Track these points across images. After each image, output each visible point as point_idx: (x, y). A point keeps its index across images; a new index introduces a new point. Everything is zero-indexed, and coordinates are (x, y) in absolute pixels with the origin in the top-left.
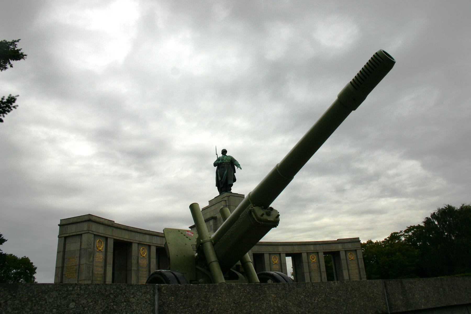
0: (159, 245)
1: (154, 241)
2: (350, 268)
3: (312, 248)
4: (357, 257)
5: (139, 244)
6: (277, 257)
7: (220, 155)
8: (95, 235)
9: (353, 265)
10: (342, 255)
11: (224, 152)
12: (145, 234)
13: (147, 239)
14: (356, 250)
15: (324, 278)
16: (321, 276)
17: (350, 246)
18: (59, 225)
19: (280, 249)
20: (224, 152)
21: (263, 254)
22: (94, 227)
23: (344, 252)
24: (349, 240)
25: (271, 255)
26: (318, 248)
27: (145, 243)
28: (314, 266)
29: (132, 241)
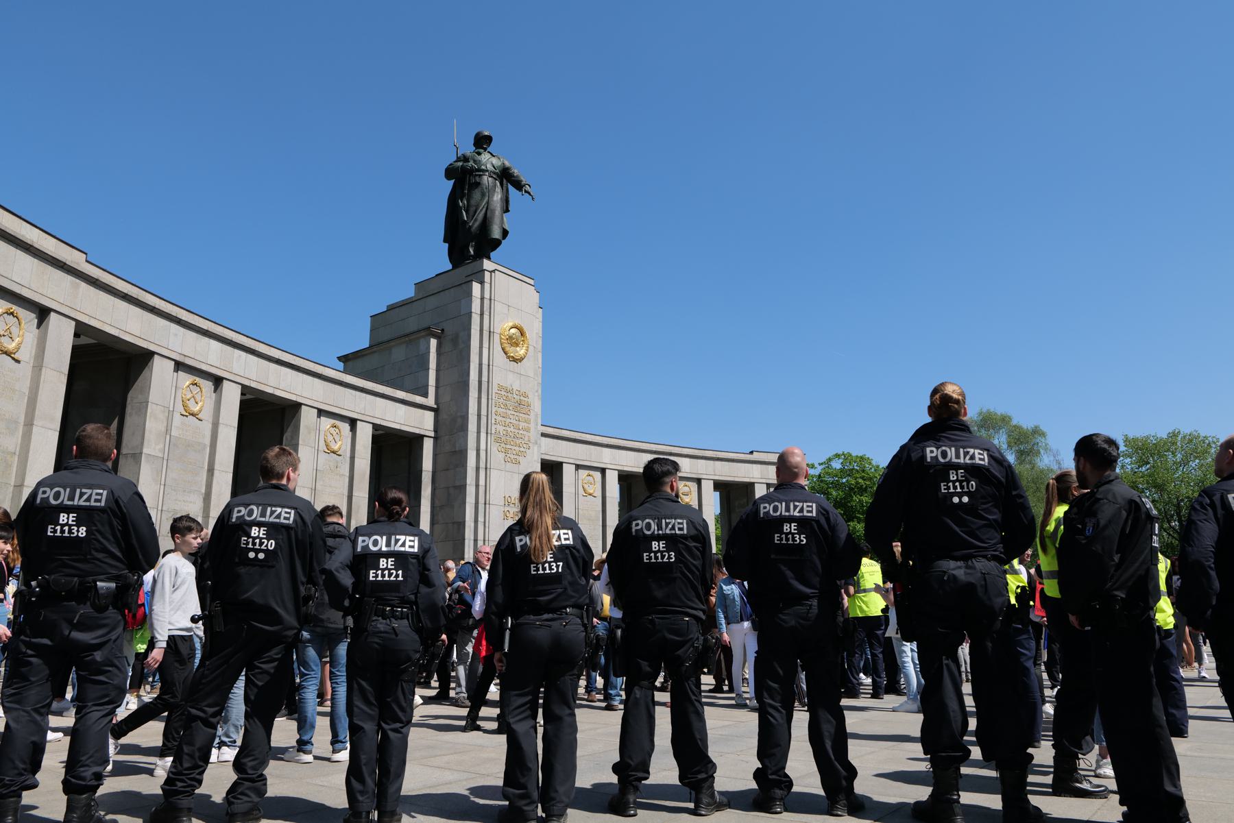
0: (254, 385)
11: (482, 141)
13: (211, 355)
20: (482, 141)
21: (561, 464)
25: (580, 471)
27: (204, 367)
29: (152, 348)
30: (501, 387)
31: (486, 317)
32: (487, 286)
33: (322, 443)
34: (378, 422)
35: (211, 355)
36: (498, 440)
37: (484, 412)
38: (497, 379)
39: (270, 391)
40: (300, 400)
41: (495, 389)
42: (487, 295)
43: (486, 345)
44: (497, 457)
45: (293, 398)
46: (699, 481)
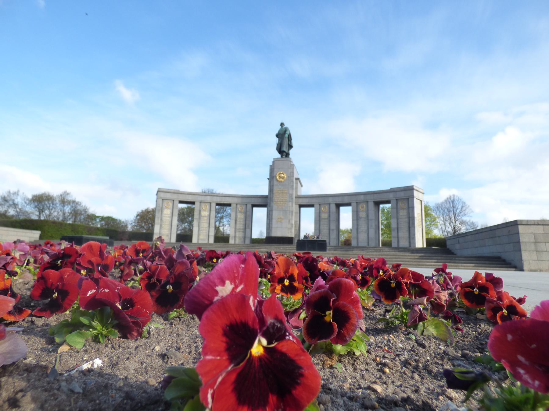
2: (400, 217)
3: (362, 198)
4: (409, 205)
5: (200, 202)
6: (327, 207)
7: (280, 127)
8: (163, 199)
11: (282, 124)
13: (208, 199)
14: (408, 199)
16: (368, 224)
17: (402, 195)
19: (330, 200)
22: (162, 195)
23: (395, 201)
26: (368, 197)
28: (362, 214)
44: (275, 207)
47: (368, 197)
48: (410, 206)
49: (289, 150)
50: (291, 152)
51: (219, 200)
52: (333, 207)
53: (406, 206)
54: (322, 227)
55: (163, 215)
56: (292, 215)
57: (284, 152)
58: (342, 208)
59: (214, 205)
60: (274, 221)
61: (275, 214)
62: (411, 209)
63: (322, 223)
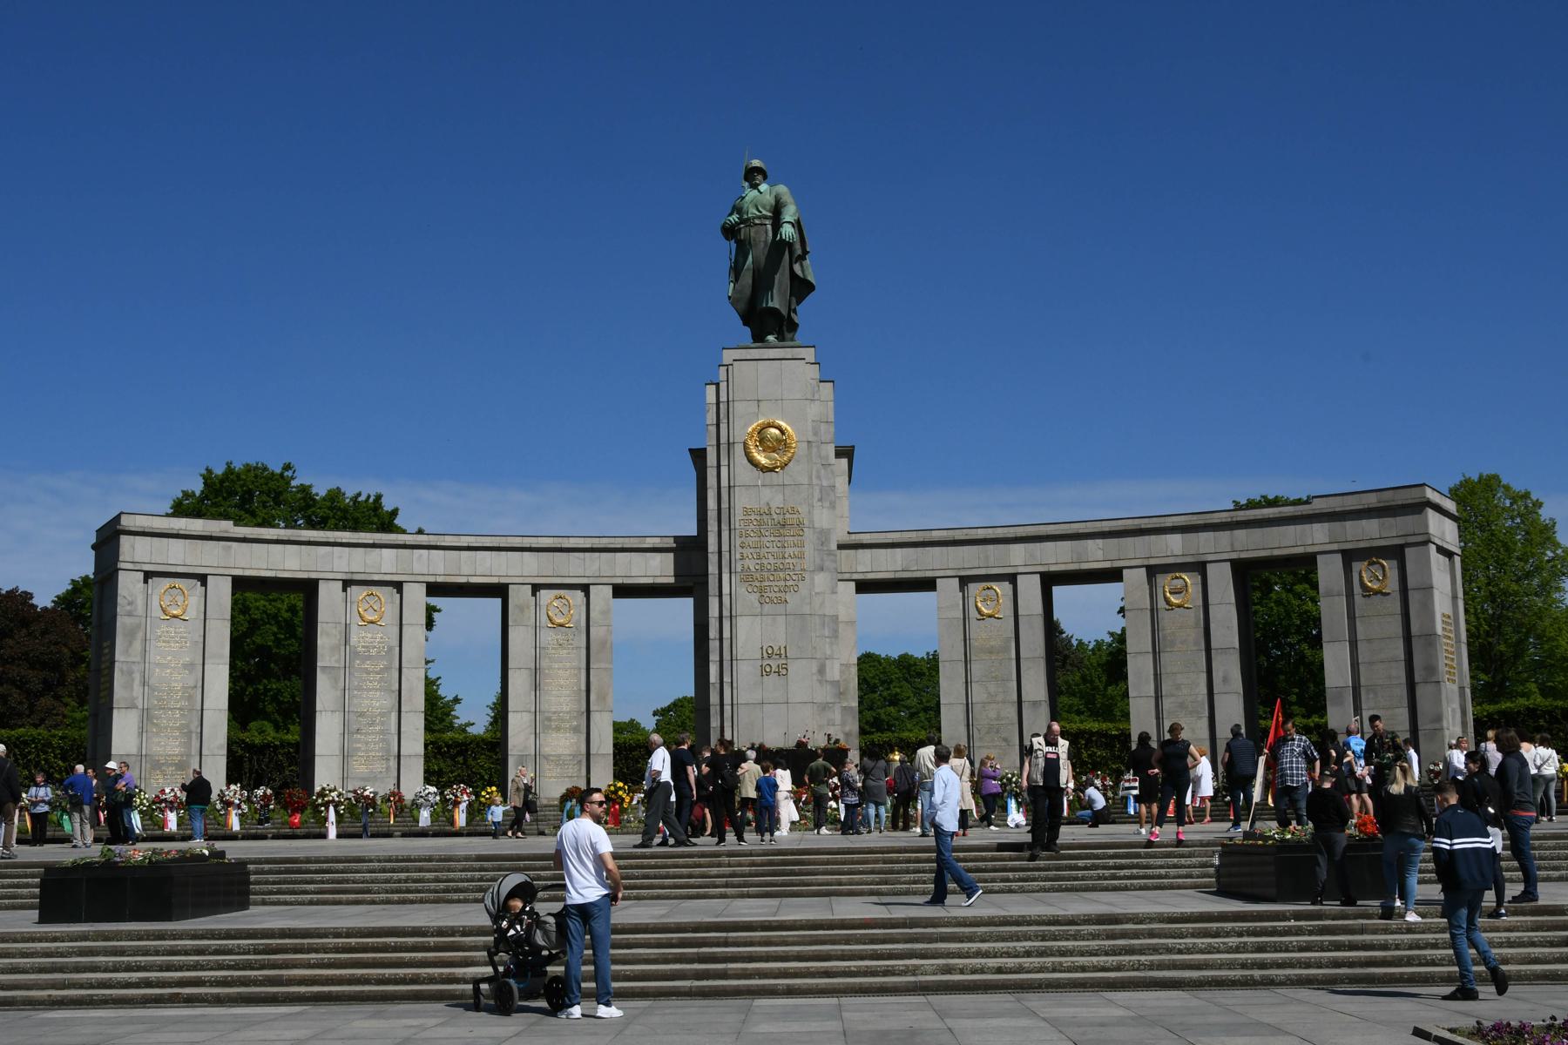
0: (440, 579)
1: (417, 568)
3: (1173, 547)
5: (347, 584)
8: (148, 575)
9: (1381, 624)
10: (1329, 572)
12: (374, 546)
13: (386, 563)
15: (1225, 680)
17: (1370, 531)
18: (94, 547)
24: (1371, 501)
25: (974, 588)
27: (376, 578)
29: (314, 576)
30: (746, 511)
31: (723, 427)
32: (723, 386)
33: (544, 618)
34: (619, 581)
35: (386, 563)
36: (748, 578)
37: (725, 547)
38: (742, 500)
39: (463, 580)
40: (503, 580)
41: (738, 515)
42: (723, 398)
43: (724, 462)
45: (495, 580)
46: (1200, 568)
47: (1205, 544)
48: (1411, 583)
49: (791, 310)
50: (805, 313)
51: (441, 566)
52: (1030, 589)
53: (1392, 584)
54: (978, 694)
55: (154, 657)
56: (835, 635)
57: (774, 312)
58: (1058, 591)
59: (416, 597)
60: (746, 672)
61: (750, 632)
62: (1414, 598)
63: (976, 668)
